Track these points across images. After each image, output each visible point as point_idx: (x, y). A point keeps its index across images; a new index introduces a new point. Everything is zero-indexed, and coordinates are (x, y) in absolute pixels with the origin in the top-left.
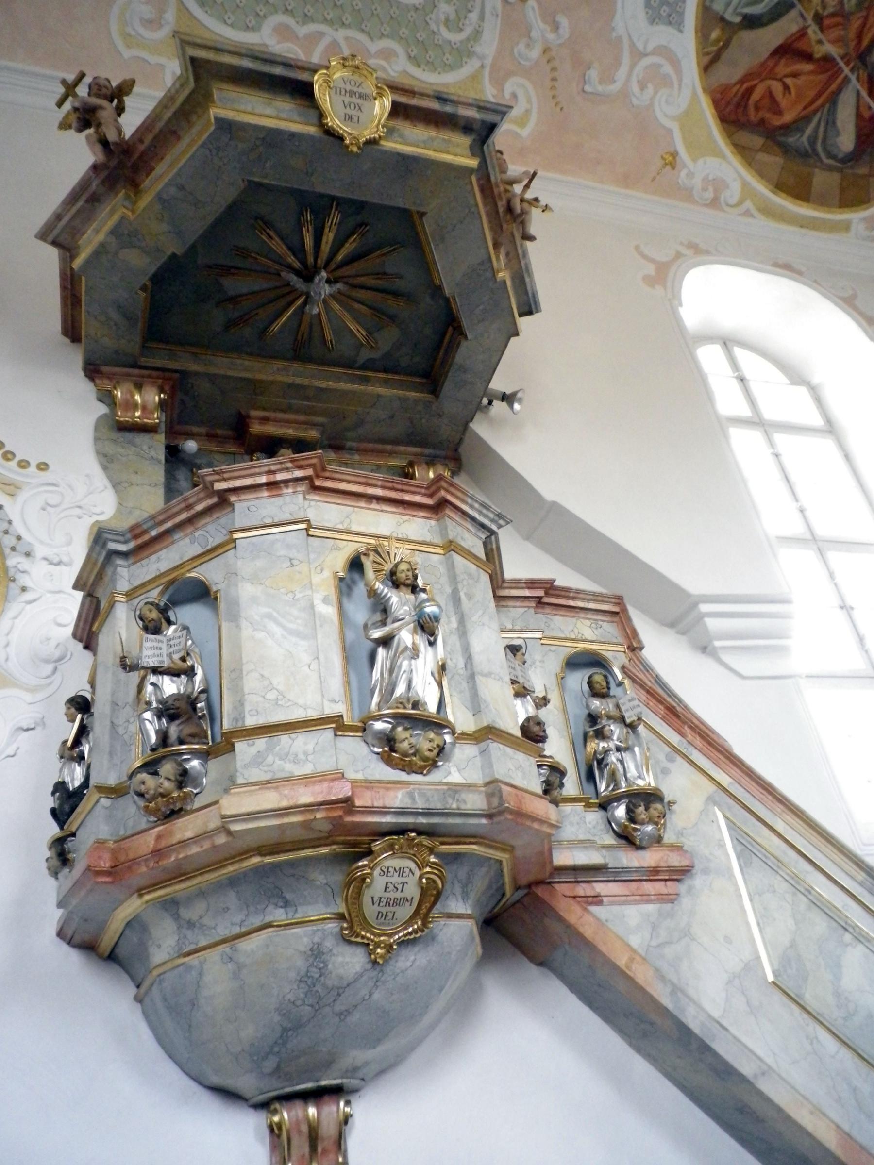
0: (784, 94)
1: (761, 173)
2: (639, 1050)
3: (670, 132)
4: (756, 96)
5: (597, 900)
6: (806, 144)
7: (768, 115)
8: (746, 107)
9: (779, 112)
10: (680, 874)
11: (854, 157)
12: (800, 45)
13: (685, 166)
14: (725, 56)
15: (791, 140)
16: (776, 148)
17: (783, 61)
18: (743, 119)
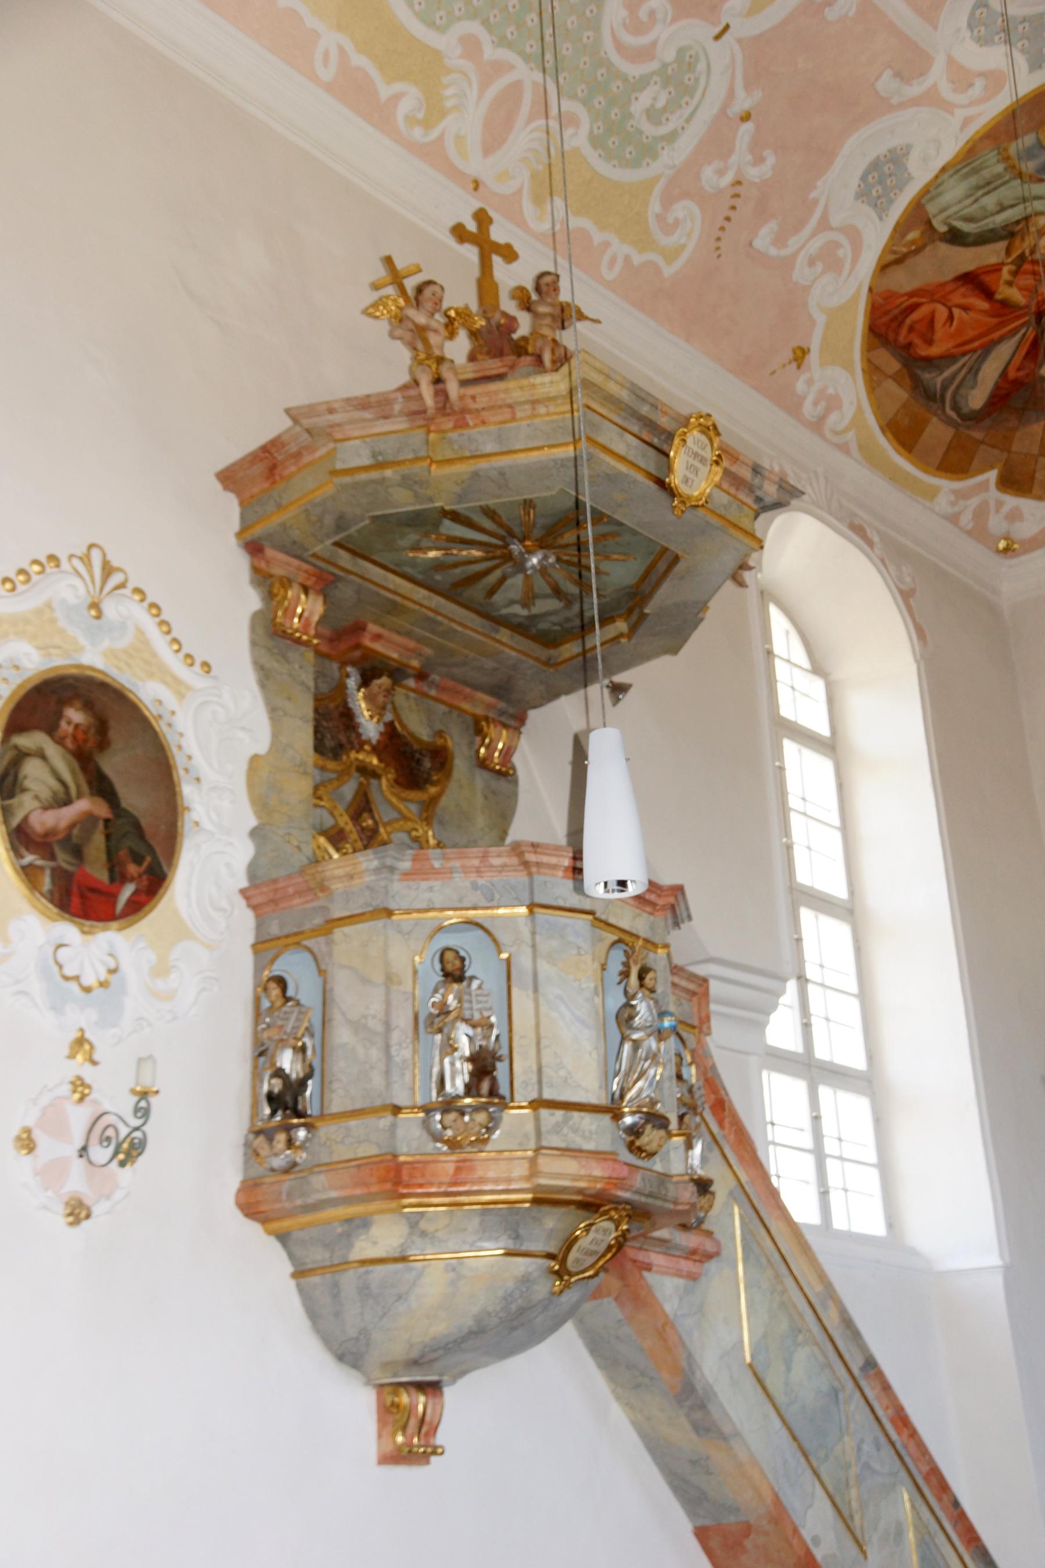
0: (945, 324)
1: (878, 408)
3: (813, 322)
4: (915, 316)
6: (939, 386)
7: (917, 341)
8: (900, 325)
11: (975, 418)
12: (987, 279)
14: (910, 262)
15: (926, 376)
16: (907, 380)
17: (962, 290)
18: (891, 336)
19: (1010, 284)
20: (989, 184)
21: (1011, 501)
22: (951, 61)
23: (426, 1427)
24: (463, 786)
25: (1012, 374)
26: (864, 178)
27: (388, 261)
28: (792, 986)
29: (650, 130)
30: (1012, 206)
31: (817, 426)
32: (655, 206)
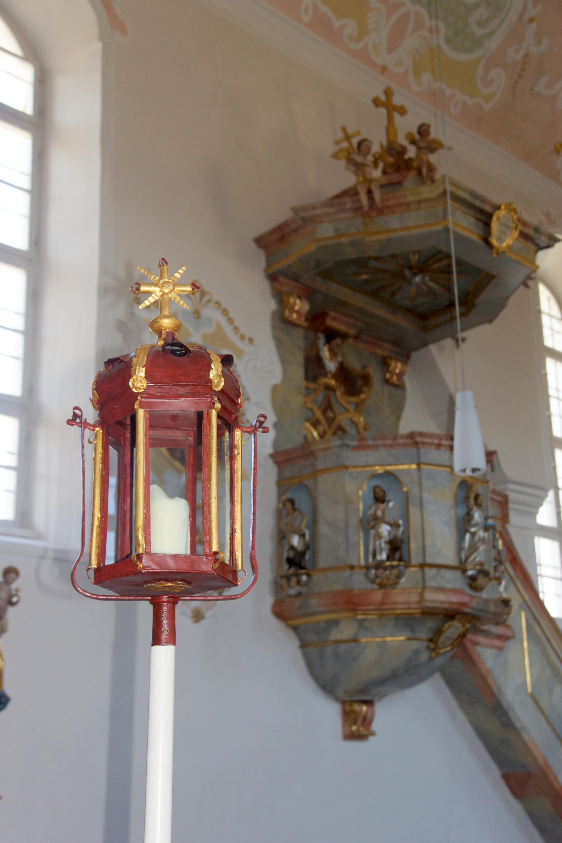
2: (462, 708)
5: (477, 644)
10: (506, 638)
23: (367, 721)
24: (377, 393)
27: (344, 129)
28: (551, 494)
29: (478, 31)
32: (480, 72)
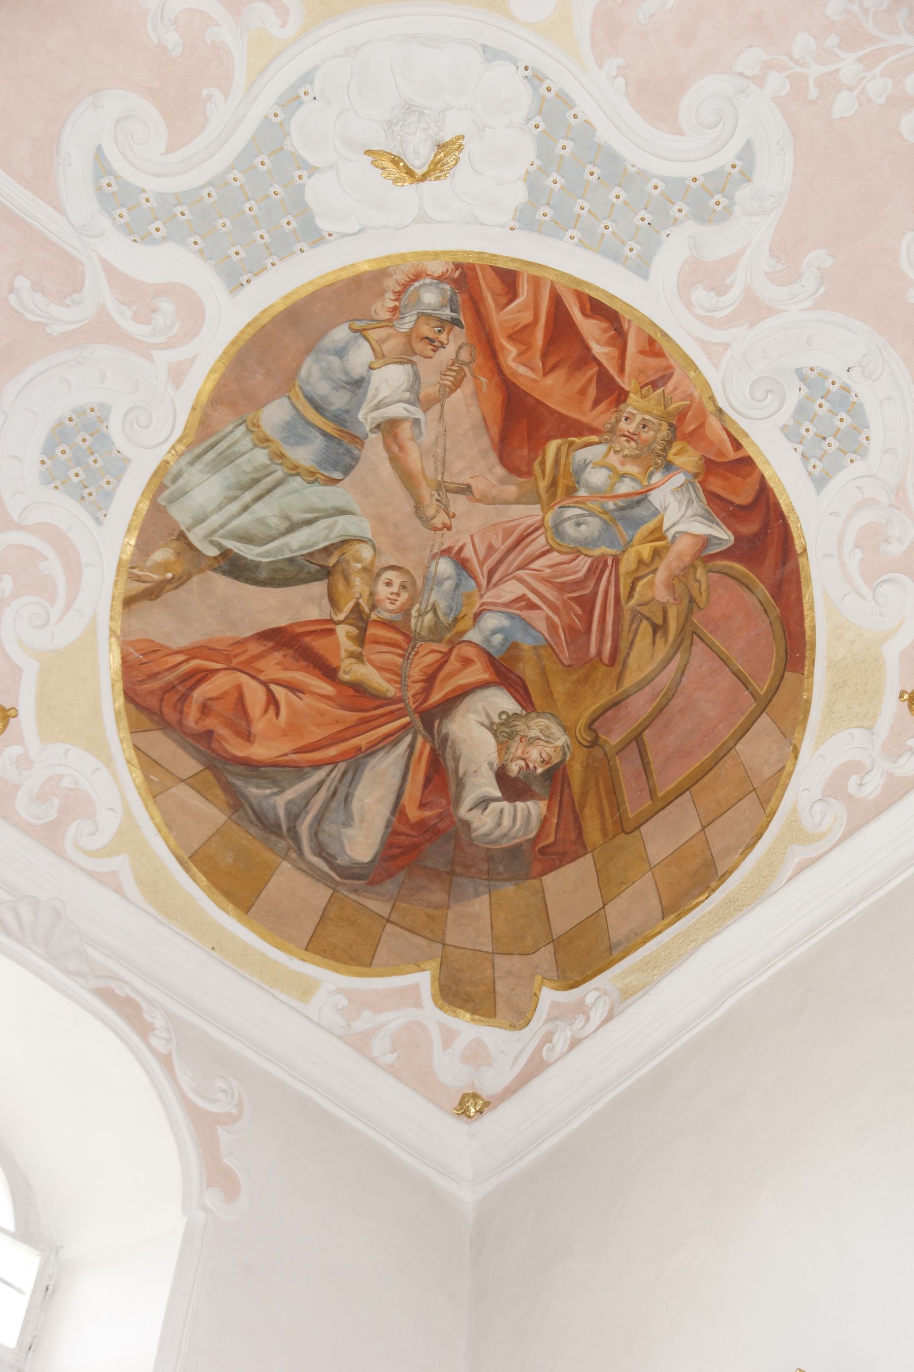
0: (266, 711)
1: (170, 824)
3: (16, 671)
6: (282, 813)
7: (222, 731)
8: (184, 698)
9: (248, 737)
12: (319, 645)
13: (20, 741)
14: (169, 596)
15: (253, 791)
16: (219, 791)
17: (278, 655)
18: (170, 714)
19: (358, 657)
20: (256, 481)
21: (466, 1028)
22: (110, 270)
25: (414, 814)
26: (48, 449)
30: (309, 522)
31: (49, 835)
